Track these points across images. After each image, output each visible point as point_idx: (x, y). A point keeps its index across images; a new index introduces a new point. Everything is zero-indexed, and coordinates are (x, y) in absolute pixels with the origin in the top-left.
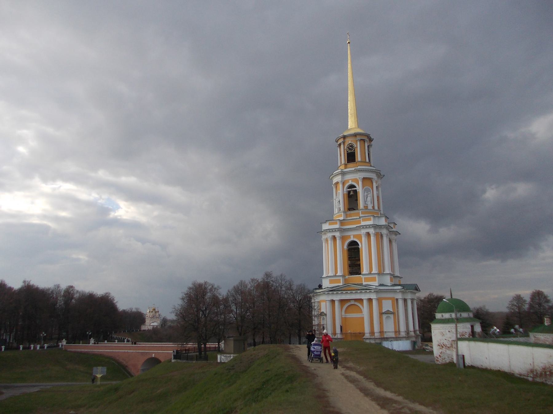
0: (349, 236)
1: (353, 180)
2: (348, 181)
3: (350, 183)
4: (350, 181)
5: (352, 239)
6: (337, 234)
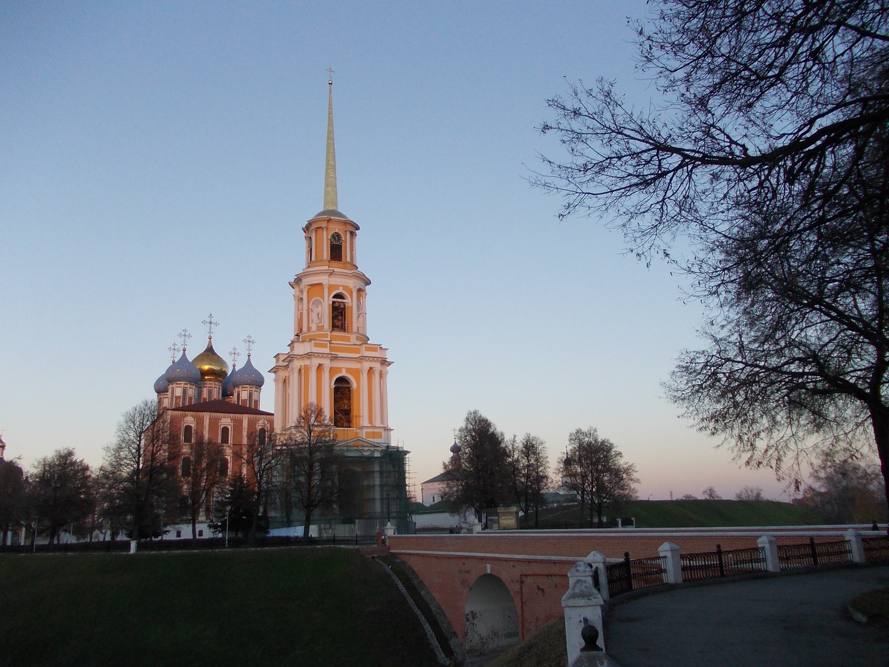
0: (339, 370)
1: (346, 288)
2: (337, 287)
3: (340, 290)
4: (341, 288)
5: (344, 374)
6: (327, 363)
